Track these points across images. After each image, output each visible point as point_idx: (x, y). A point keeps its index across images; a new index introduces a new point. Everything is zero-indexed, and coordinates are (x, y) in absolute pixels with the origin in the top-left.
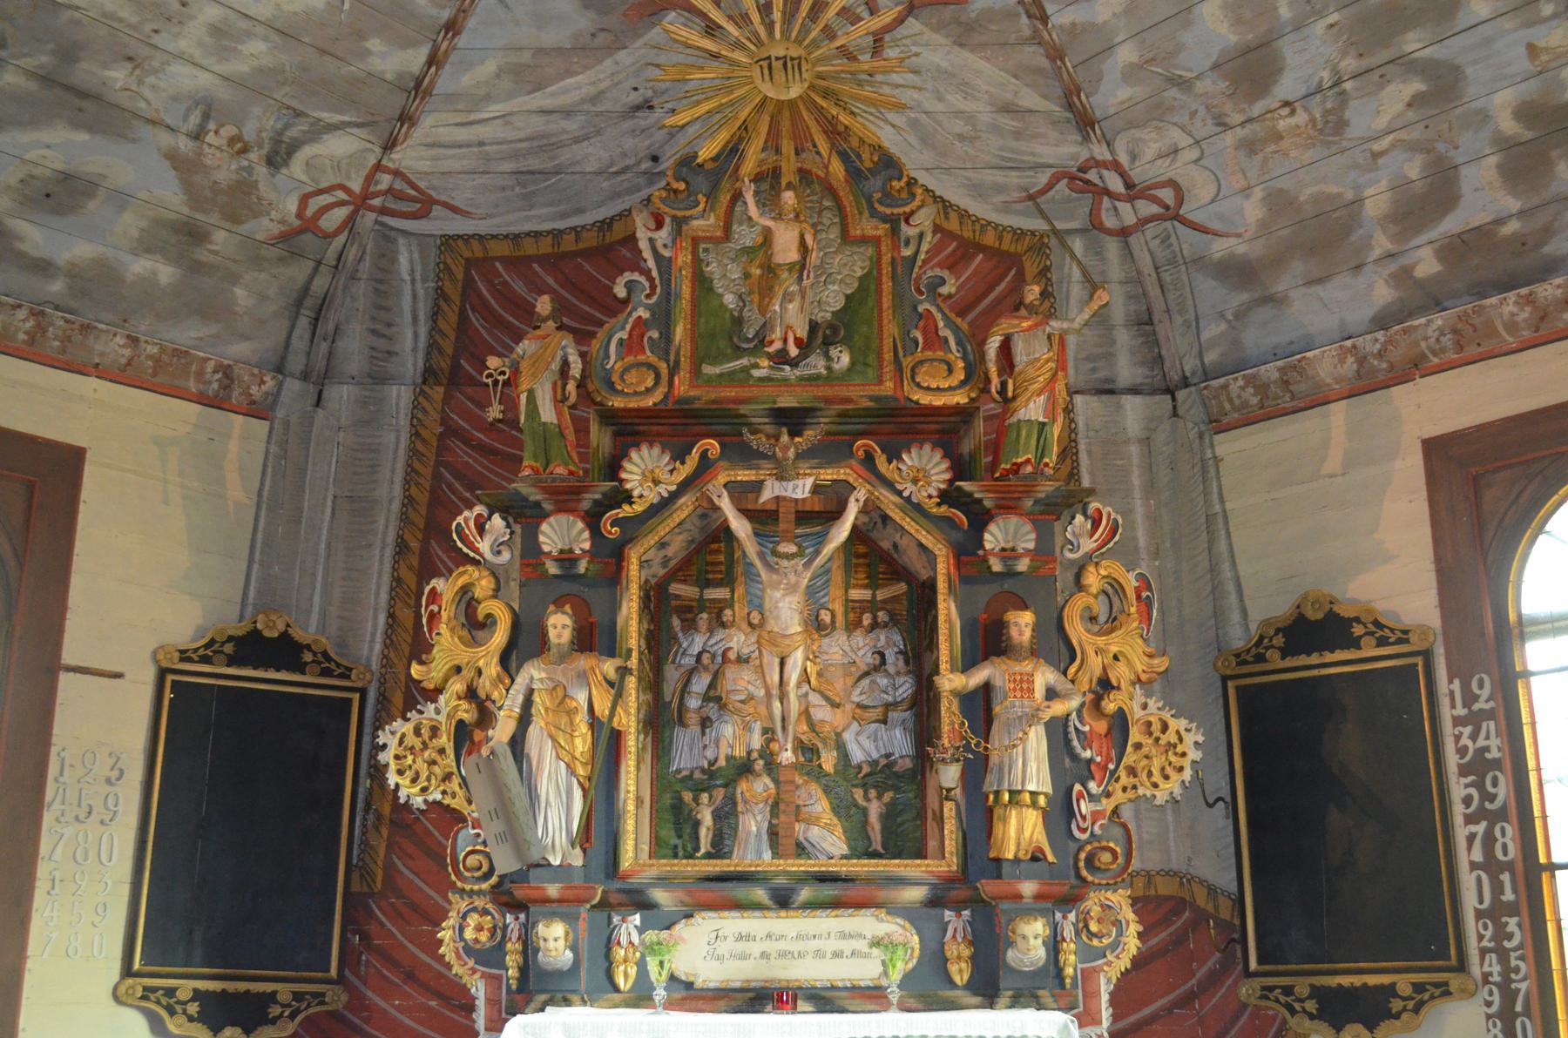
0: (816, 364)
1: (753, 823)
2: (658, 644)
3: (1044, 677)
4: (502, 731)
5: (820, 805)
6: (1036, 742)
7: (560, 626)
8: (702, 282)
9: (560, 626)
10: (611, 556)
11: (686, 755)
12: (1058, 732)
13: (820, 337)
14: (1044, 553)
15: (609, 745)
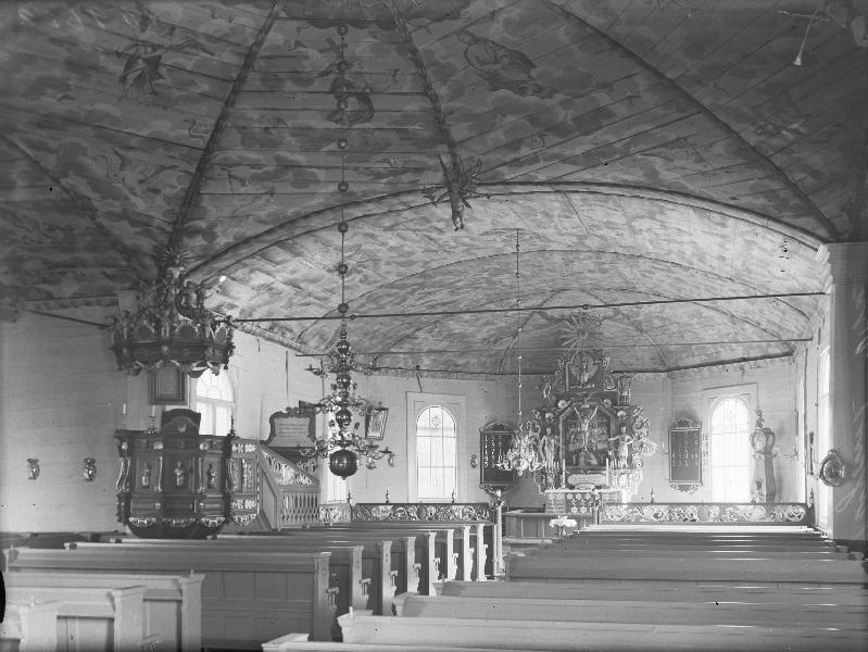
0: (589, 386)
1: (582, 459)
2: (566, 430)
3: (627, 437)
4: (540, 447)
5: (593, 457)
6: (626, 448)
7: (549, 430)
8: (570, 372)
9: (549, 430)
10: (557, 418)
11: (571, 448)
12: (630, 446)
13: (590, 381)
14: (628, 415)
15: (557, 449)
